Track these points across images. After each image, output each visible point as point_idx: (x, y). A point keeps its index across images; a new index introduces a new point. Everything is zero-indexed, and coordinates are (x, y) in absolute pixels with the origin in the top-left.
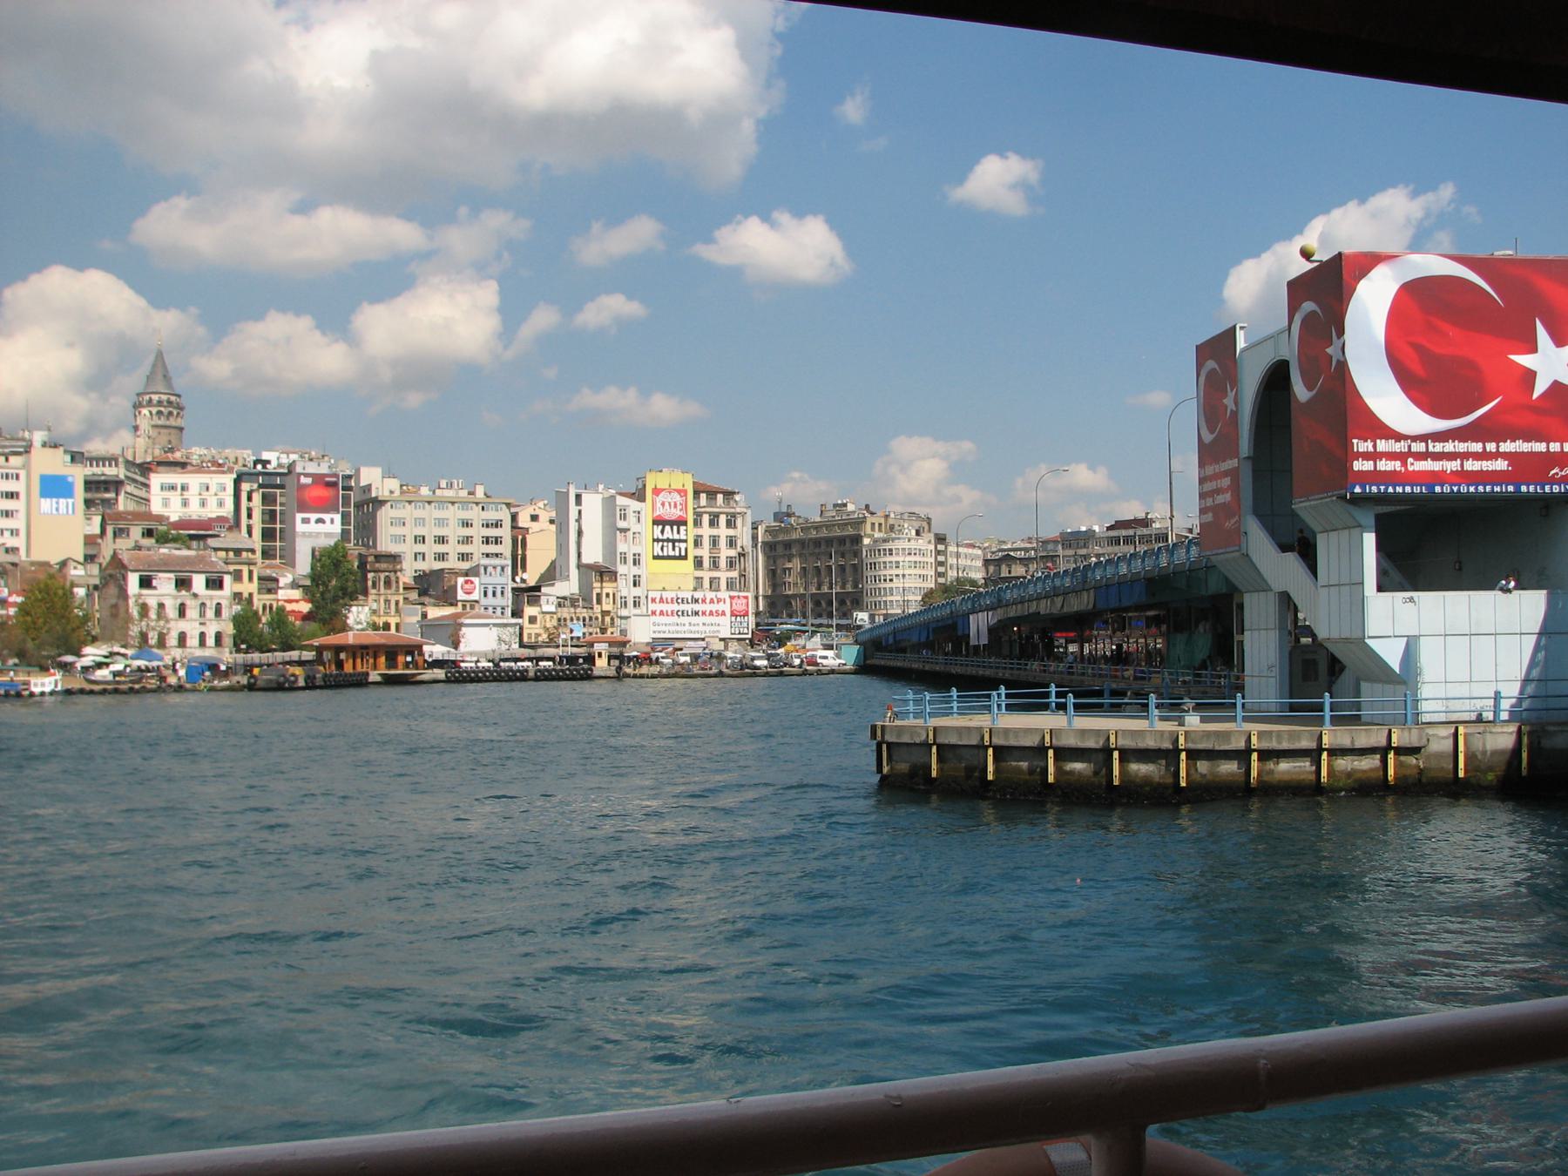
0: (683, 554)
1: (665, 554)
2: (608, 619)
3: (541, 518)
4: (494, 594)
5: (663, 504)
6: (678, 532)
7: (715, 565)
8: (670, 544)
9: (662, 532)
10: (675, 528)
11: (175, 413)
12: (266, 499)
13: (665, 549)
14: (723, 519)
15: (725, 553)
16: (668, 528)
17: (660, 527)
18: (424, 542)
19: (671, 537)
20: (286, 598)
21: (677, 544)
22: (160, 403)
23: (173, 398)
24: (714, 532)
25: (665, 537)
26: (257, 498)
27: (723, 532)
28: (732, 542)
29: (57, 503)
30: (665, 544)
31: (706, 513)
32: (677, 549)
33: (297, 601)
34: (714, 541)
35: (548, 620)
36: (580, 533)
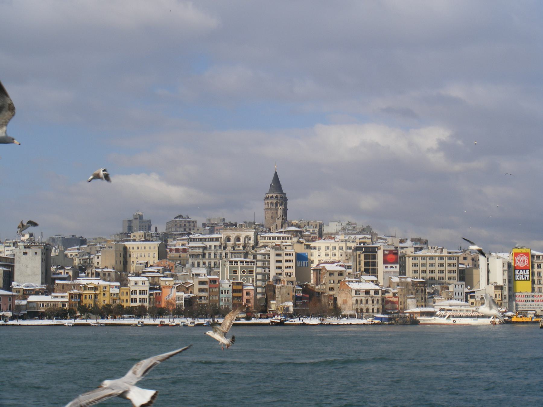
0: (528, 279)
1: (520, 279)
2: (500, 303)
3: (468, 258)
4: (459, 294)
5: (519, 261)
6: (526, 272)
8: (522, 276)
9: (519, 272)
12: (366, 257)
13: (520, 278)
18: (425, 273)
19: (522, 274)
20: (388, 296)
21: (525, 276)
22: (277, 197)
25: (520, 274)
26: (362, 256)
29: (302, 263)
30: (520, 276)
31: (536, 263)
32: (525, 278)
33: (392, 297)
35: (478, 304)
36: (488, 272)
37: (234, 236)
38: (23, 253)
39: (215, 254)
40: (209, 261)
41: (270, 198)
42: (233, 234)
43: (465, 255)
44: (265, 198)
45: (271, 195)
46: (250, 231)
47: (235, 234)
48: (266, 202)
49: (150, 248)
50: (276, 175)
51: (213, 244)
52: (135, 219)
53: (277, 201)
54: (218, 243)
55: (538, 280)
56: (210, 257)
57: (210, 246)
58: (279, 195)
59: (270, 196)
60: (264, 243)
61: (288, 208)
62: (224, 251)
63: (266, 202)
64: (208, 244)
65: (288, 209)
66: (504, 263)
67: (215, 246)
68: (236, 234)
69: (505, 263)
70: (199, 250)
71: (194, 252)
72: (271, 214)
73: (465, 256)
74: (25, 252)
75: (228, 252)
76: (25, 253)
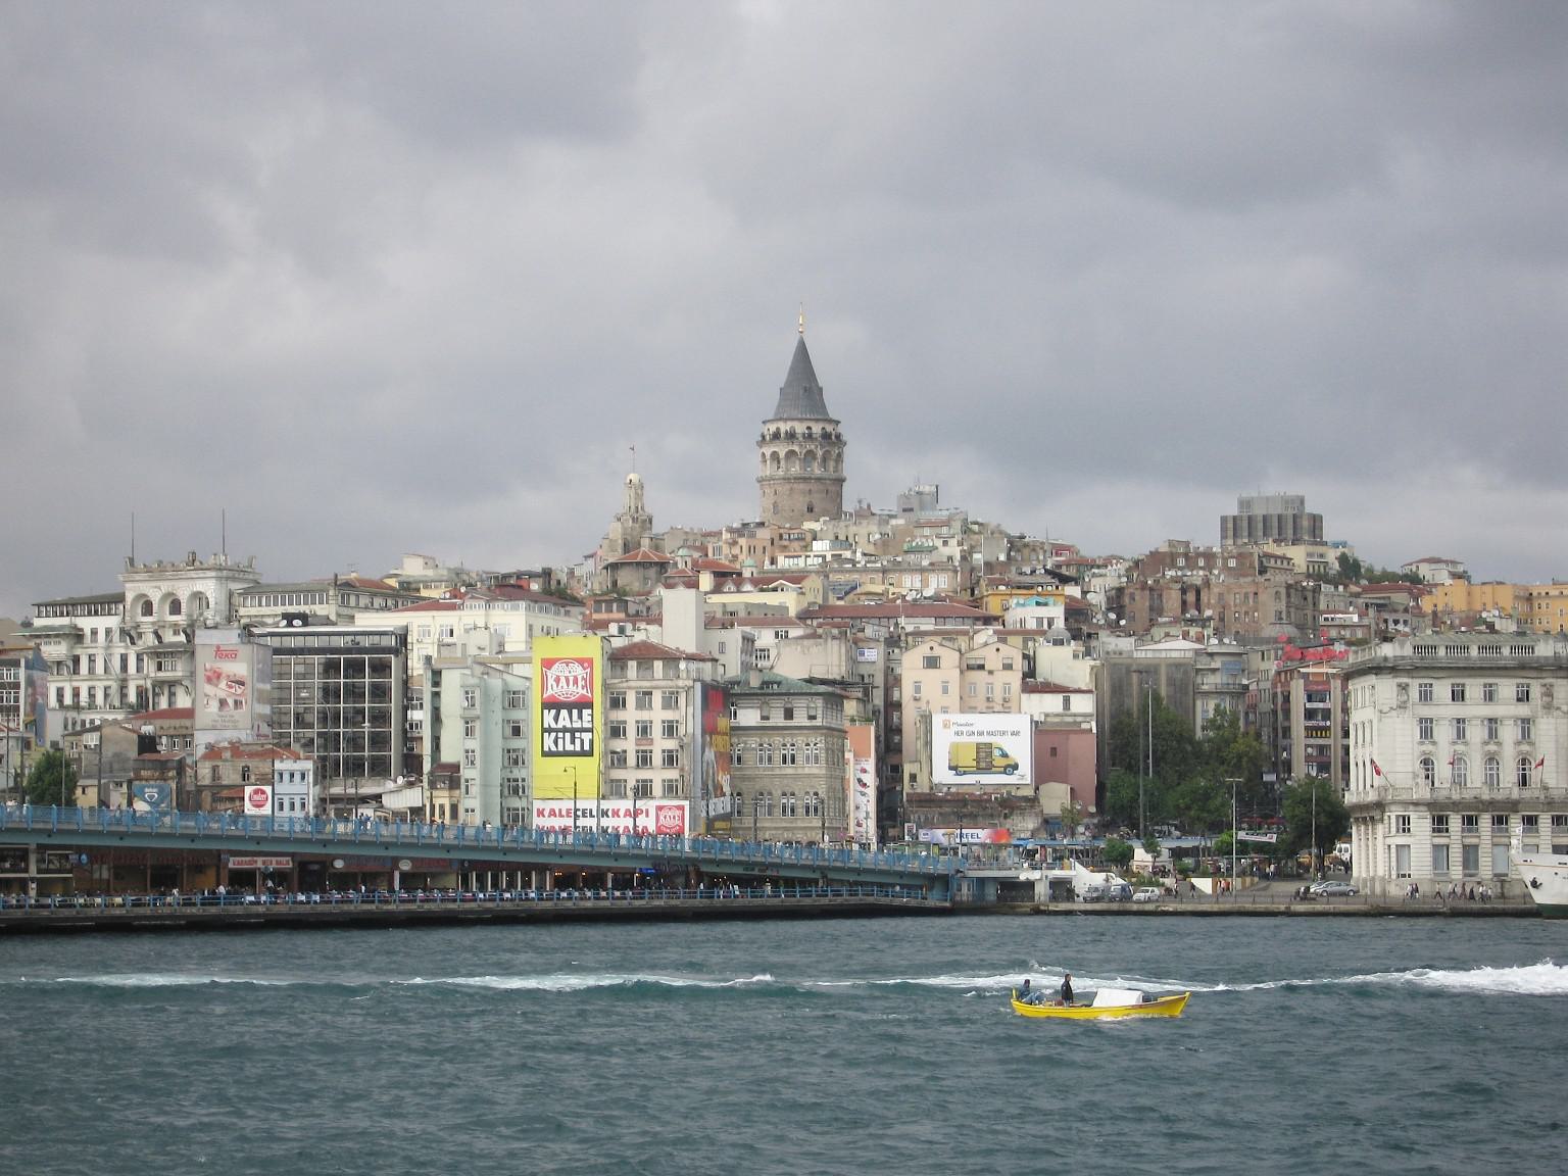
0: (587, 747)
1: (561, 748)
3: (943, 663)
5: (558, 680)
6: (580, 717)
7: (644, 760)
8: (568, 735)
9: (556, 719)
10: (575, 712)
11: (820, 453)
13: (560, 742)
14: (657, 698)
15: (660, 744)
16: (564, 713)
17: (553, 712)
19: (569, 725)
21: (577, 735)
24: (645, 715)
25: (560, 726)
27: (658, 715)
28: (670, 729)
30: (560, 735)
32: (578, 741)
34: (644, 730)
40: (91, 683)
43: (932, 648)
44: (763, 437)
45: (784, 427)
48: (768, 453)
50: (802, 352)
51: (101, 623)
52: (905, 510)
54: (112, 622)
55: (637, 752)
57: (94, 632)
58: (817, 429)
59: (783, 431)
64: (86, 623)
65: (844, 480)
66: (467, 693)
69: (473, 692)
70: (57, 647)
72: (772, 499)
73: (929, 653)
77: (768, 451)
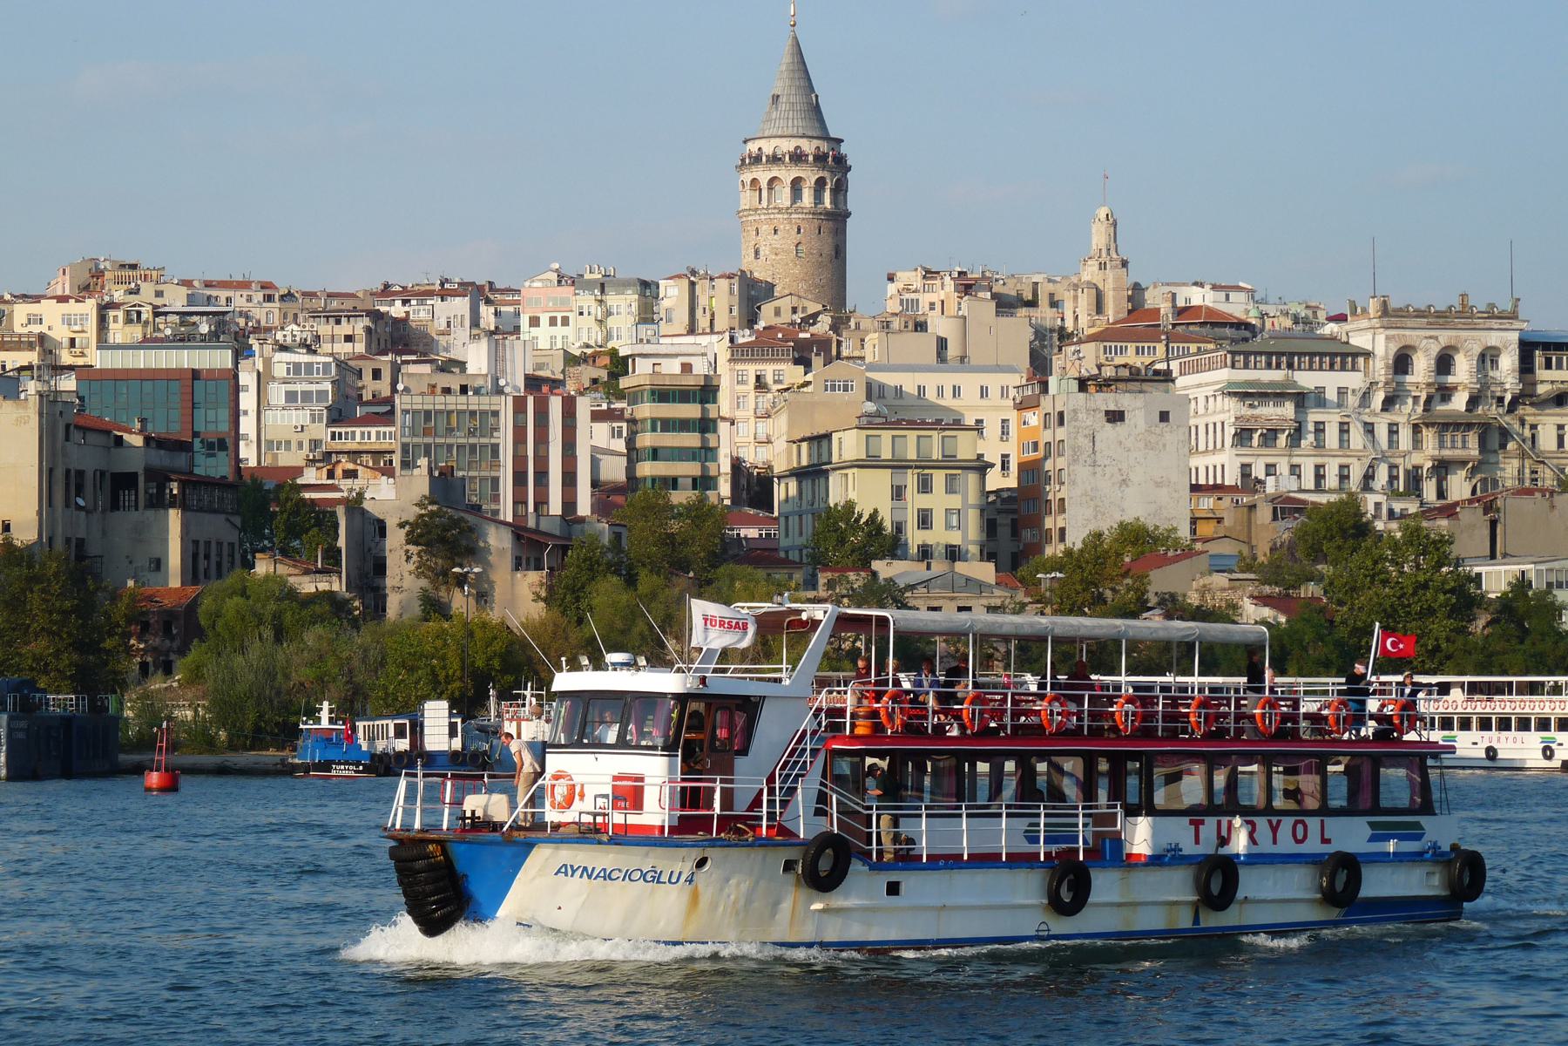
22: (797, 157)
23: (824, 147)
37: (1435, 350)
38: (1107, 413)
39: (1344, 429)
40: (1319, 460)
41: (764, 159)
42: (1431, 337)
46: (1507, 326)
47: (1436, 338)
49: (984, 392)
53: (821, 174)
54: (1353, 380)
56: (1319, 445)
60: (1552, 382)
61: (850, 207)
62: (1386, 415)
63: (747, 177)
64: (1307, 379)
67: (1342, 392)
68: (1440, 339)
71: (1256, 418)
72: (796, 238)
74: (1112, 407)
75: (1401, 419)
76: (1115, 417)
77: (787, 174)
